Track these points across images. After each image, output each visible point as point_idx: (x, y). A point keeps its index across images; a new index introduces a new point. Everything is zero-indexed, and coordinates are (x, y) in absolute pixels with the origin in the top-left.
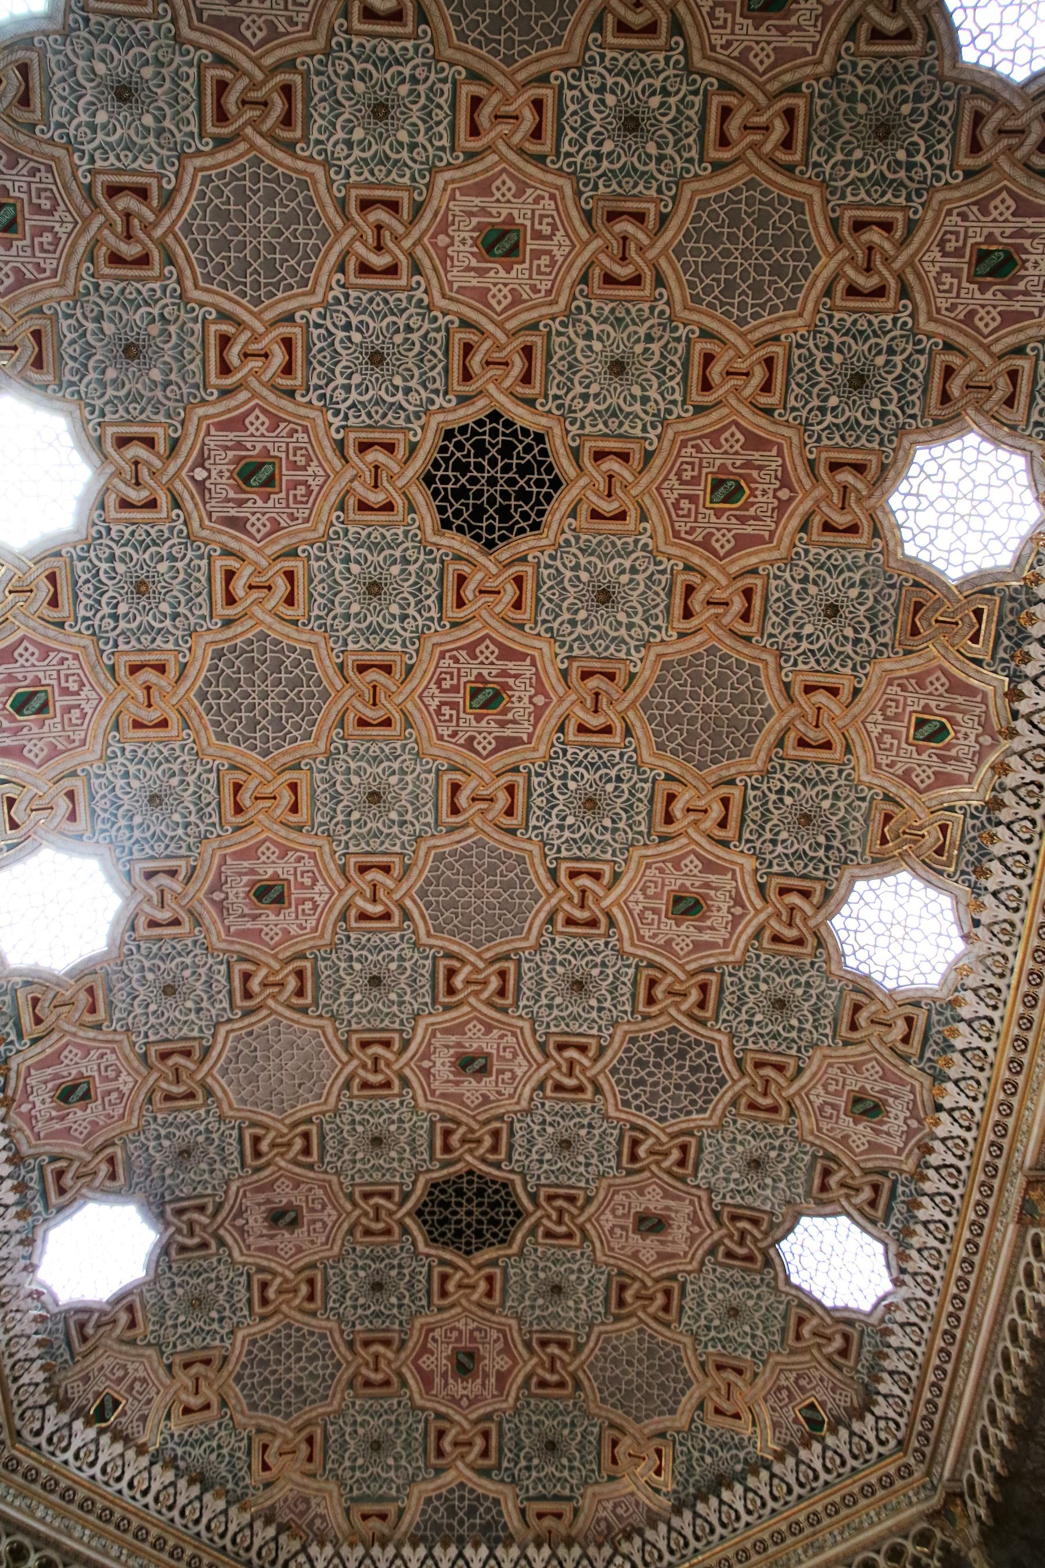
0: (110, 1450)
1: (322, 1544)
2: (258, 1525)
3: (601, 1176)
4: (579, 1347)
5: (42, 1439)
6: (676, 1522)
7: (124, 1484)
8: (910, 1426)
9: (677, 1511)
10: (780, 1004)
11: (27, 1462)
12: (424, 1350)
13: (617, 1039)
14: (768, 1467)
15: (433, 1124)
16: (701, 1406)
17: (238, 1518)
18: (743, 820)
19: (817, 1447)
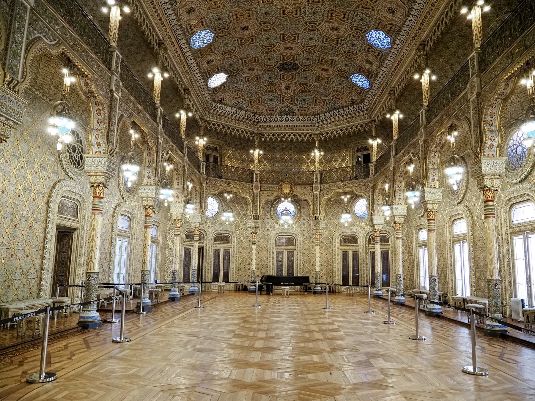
0: (224, 107)
1: (262, 115)
2: (251, 114)
3: (315, 63)
4: (310, 86)
5: (213, 107)
6: (325, 114)
7: (228, 112)
8: (369, 107)
9: (326, 112)
10: (353, 45)
11: (211, 112)
12: (280, 86)
13: (319, 46)
14: (343, 108)
15: (281, 56)
16: (333, 96)
17: (248, 113)
18: (348, 18)
19: (352, 107)
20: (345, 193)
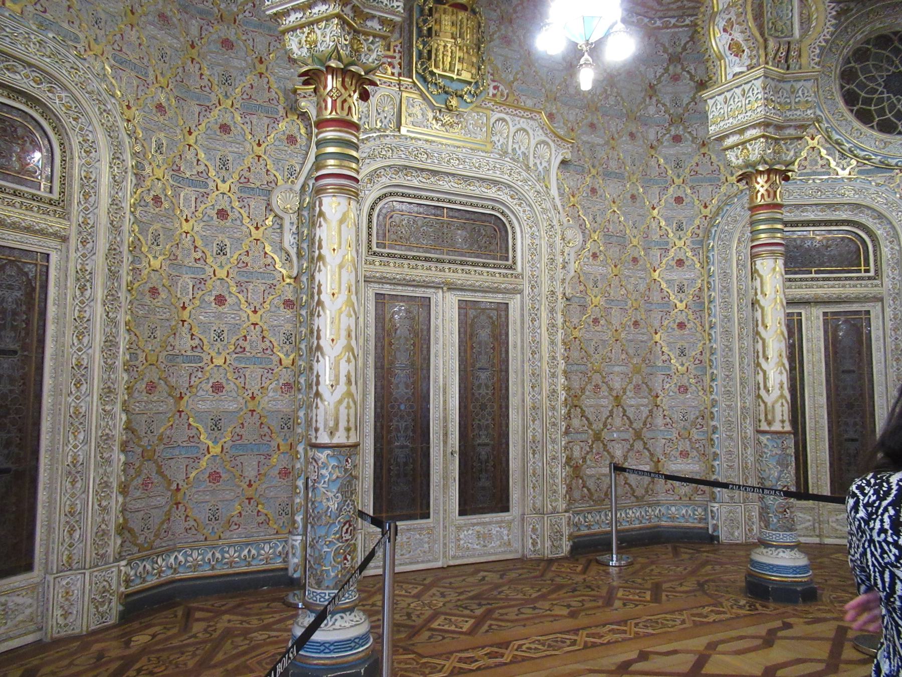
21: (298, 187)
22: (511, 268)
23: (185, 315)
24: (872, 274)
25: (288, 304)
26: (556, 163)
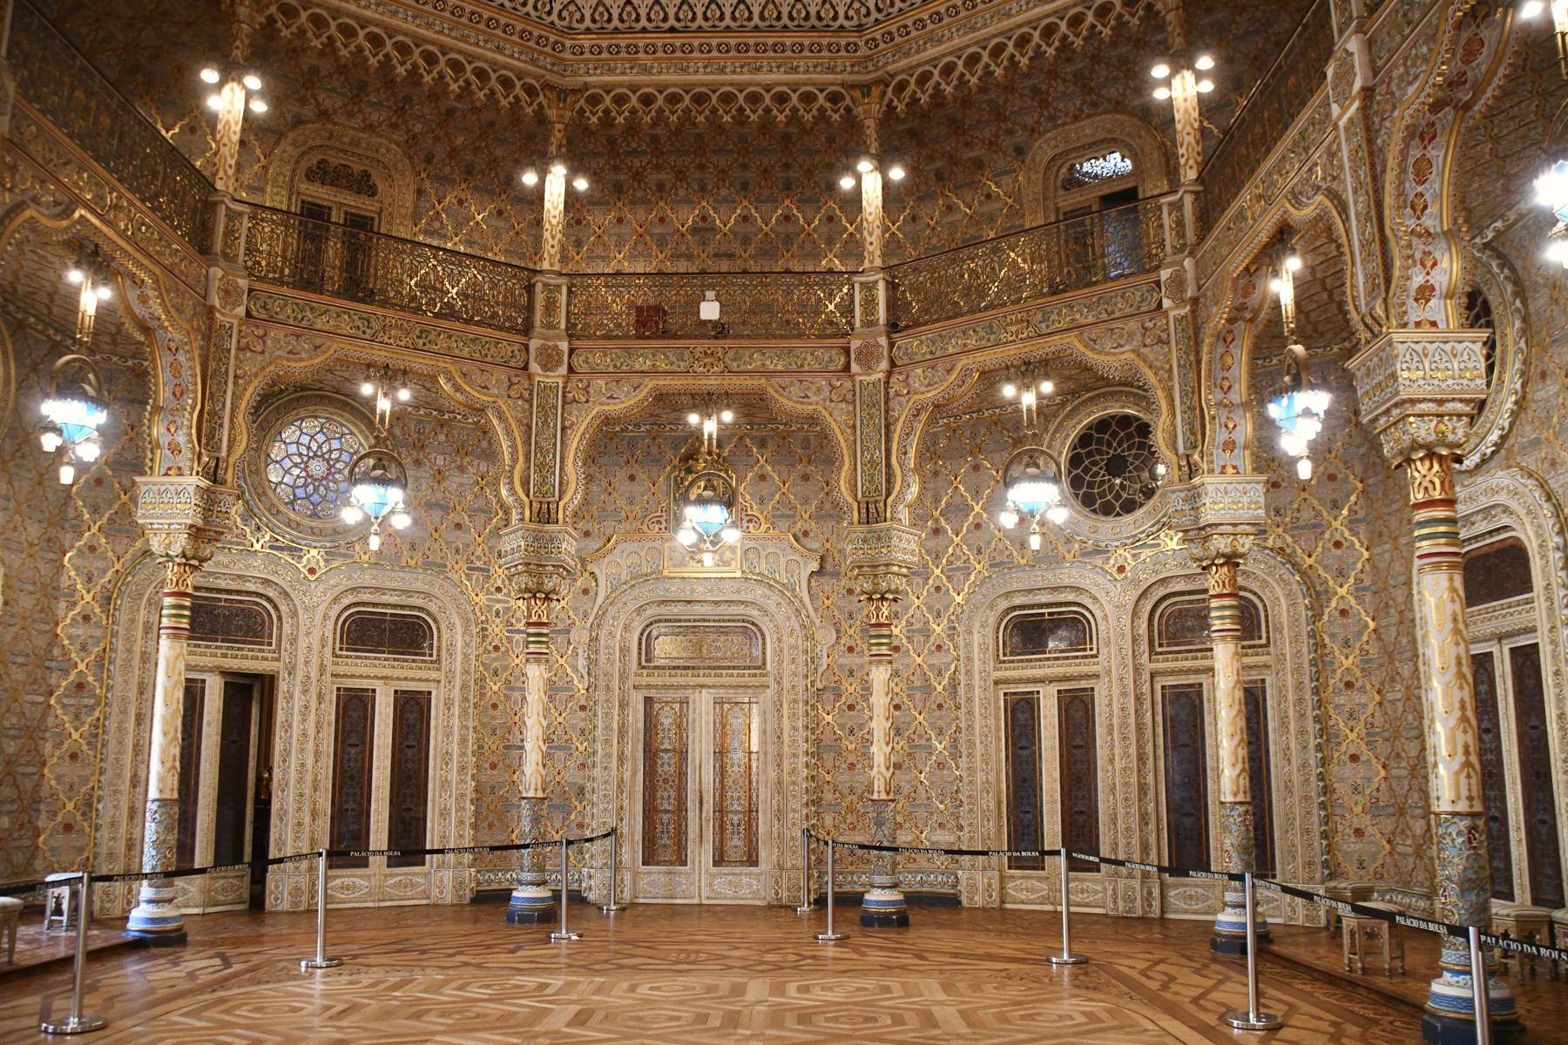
20: (1028, 372)
21: (588, 625)
22: (759, 668)
23: (517, 719)
24: (1094, 652)
25: (583, 708)
26: (805, 576)
